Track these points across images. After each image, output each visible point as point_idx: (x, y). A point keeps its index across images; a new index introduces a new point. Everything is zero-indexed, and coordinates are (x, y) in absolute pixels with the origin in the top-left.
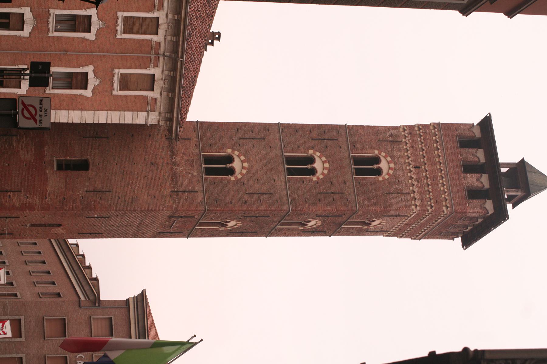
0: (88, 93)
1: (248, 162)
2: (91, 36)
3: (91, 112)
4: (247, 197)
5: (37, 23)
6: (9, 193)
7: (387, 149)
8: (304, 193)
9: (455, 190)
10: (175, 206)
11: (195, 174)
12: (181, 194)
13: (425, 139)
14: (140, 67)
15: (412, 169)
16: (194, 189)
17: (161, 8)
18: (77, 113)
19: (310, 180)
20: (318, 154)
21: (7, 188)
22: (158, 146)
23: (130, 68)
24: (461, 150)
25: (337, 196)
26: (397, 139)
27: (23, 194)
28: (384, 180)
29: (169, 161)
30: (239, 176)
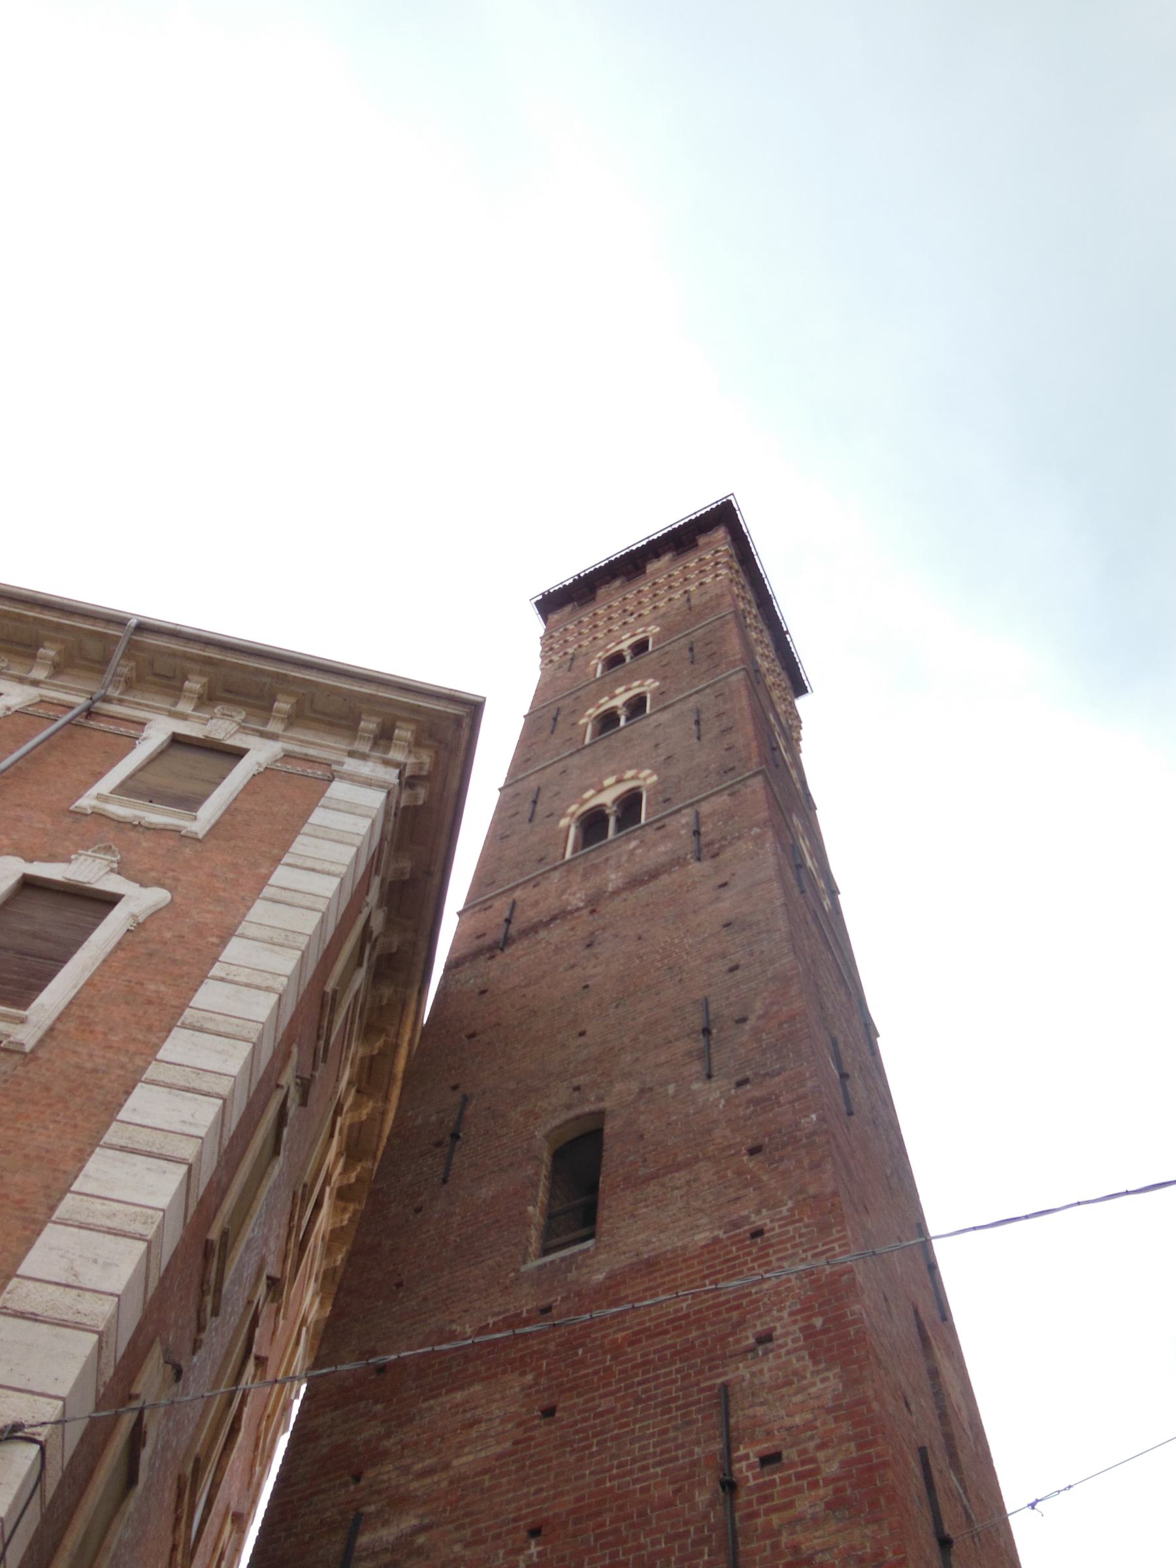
6: (745, 1470)
21: (702, 1498)
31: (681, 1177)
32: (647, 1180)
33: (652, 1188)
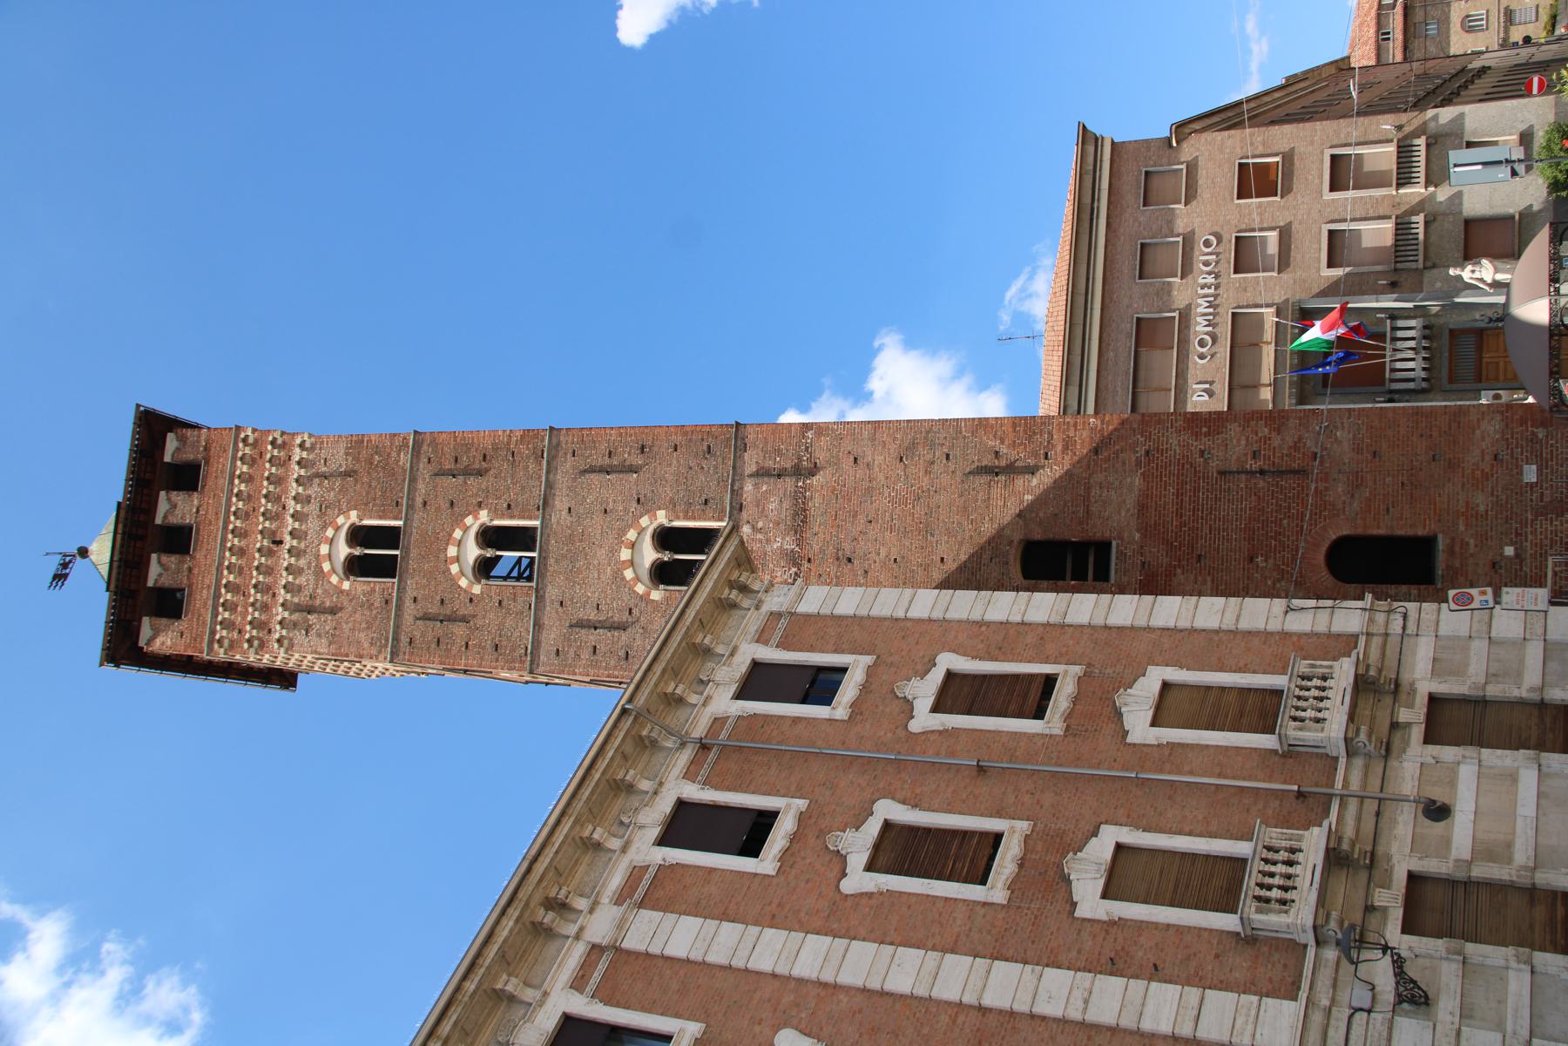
0: (949, 661)
1: (618, 562)
2: (889, 810)
5: (1060, 867)
8: (513, 477)
14: (767, 719)
15: (288, 538)
17: (636, 873)
19: (495, 513)
20: (463, 583)
21: (1261, 484)
23: (796, 720)
28: (345, 513)
30: (644, 521)
31: (1095, 492)
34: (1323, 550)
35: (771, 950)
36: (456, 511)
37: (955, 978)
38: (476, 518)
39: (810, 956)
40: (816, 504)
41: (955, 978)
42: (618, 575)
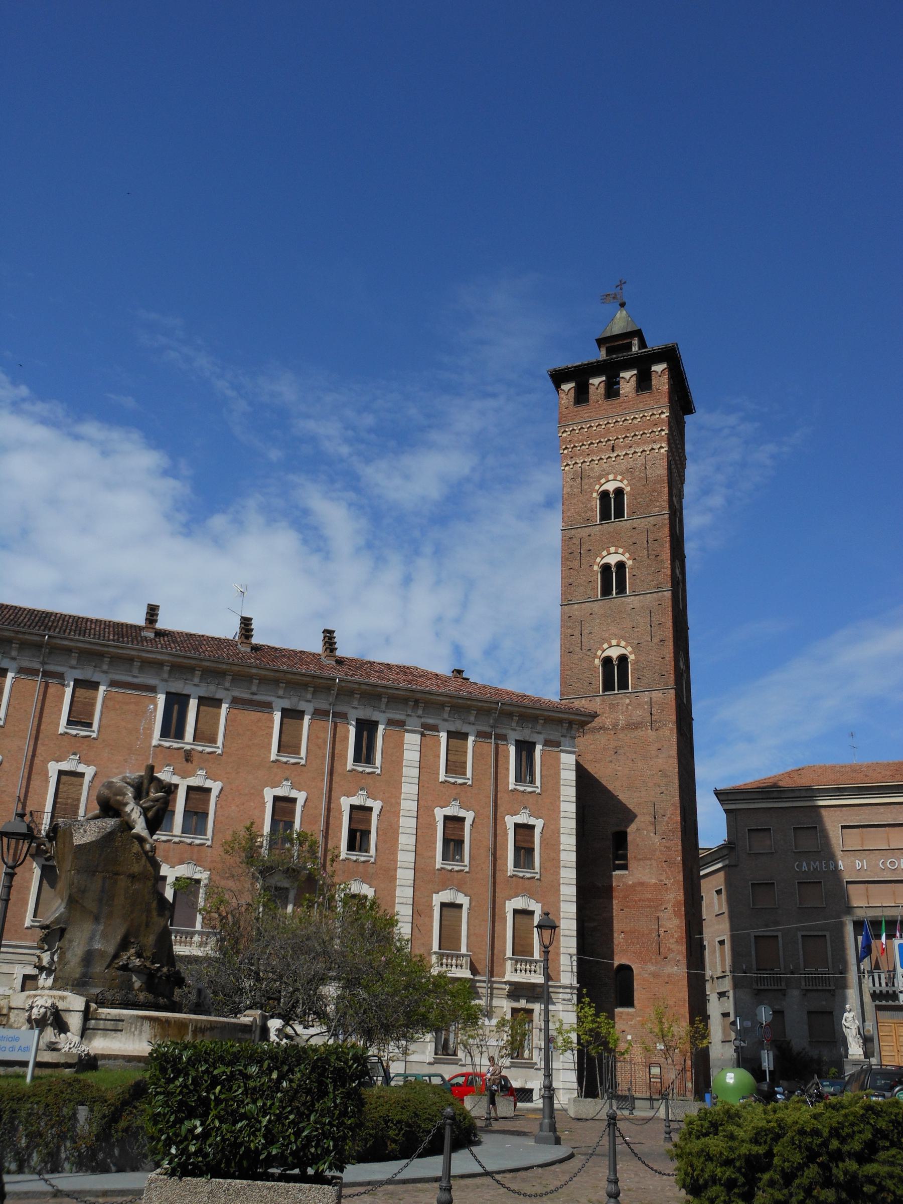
2: (469, 816)
3: (562, 821)
4: (656, 640)
6: (661, 932)
7: (591, 483)
9: (641, 405)
10: (671, 725)
11: (628, 701)
12: (654, 718)
13: (578, 441)
16: (646, 702)
18: (563, 839)
19: (632, 568)
20: (598, 560)
22: (592, 746)
24: (591, 401)
25: (650, 535)
26: (579, 473)
27: (661, 914)
28: (629, 484)
29: (612, 732)
30: (629, 649)
31: (648, 862)
32: (640, 859)
33: (641, 862)
34: (628, 963)
35: (409, 789)
36: (632, 547)
37: (405, 858)
38: (628, 559)
39: (408, 805)
40: (639, 733)
41: (405, 858)
42: (605, 640)
